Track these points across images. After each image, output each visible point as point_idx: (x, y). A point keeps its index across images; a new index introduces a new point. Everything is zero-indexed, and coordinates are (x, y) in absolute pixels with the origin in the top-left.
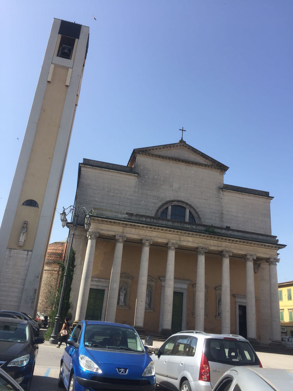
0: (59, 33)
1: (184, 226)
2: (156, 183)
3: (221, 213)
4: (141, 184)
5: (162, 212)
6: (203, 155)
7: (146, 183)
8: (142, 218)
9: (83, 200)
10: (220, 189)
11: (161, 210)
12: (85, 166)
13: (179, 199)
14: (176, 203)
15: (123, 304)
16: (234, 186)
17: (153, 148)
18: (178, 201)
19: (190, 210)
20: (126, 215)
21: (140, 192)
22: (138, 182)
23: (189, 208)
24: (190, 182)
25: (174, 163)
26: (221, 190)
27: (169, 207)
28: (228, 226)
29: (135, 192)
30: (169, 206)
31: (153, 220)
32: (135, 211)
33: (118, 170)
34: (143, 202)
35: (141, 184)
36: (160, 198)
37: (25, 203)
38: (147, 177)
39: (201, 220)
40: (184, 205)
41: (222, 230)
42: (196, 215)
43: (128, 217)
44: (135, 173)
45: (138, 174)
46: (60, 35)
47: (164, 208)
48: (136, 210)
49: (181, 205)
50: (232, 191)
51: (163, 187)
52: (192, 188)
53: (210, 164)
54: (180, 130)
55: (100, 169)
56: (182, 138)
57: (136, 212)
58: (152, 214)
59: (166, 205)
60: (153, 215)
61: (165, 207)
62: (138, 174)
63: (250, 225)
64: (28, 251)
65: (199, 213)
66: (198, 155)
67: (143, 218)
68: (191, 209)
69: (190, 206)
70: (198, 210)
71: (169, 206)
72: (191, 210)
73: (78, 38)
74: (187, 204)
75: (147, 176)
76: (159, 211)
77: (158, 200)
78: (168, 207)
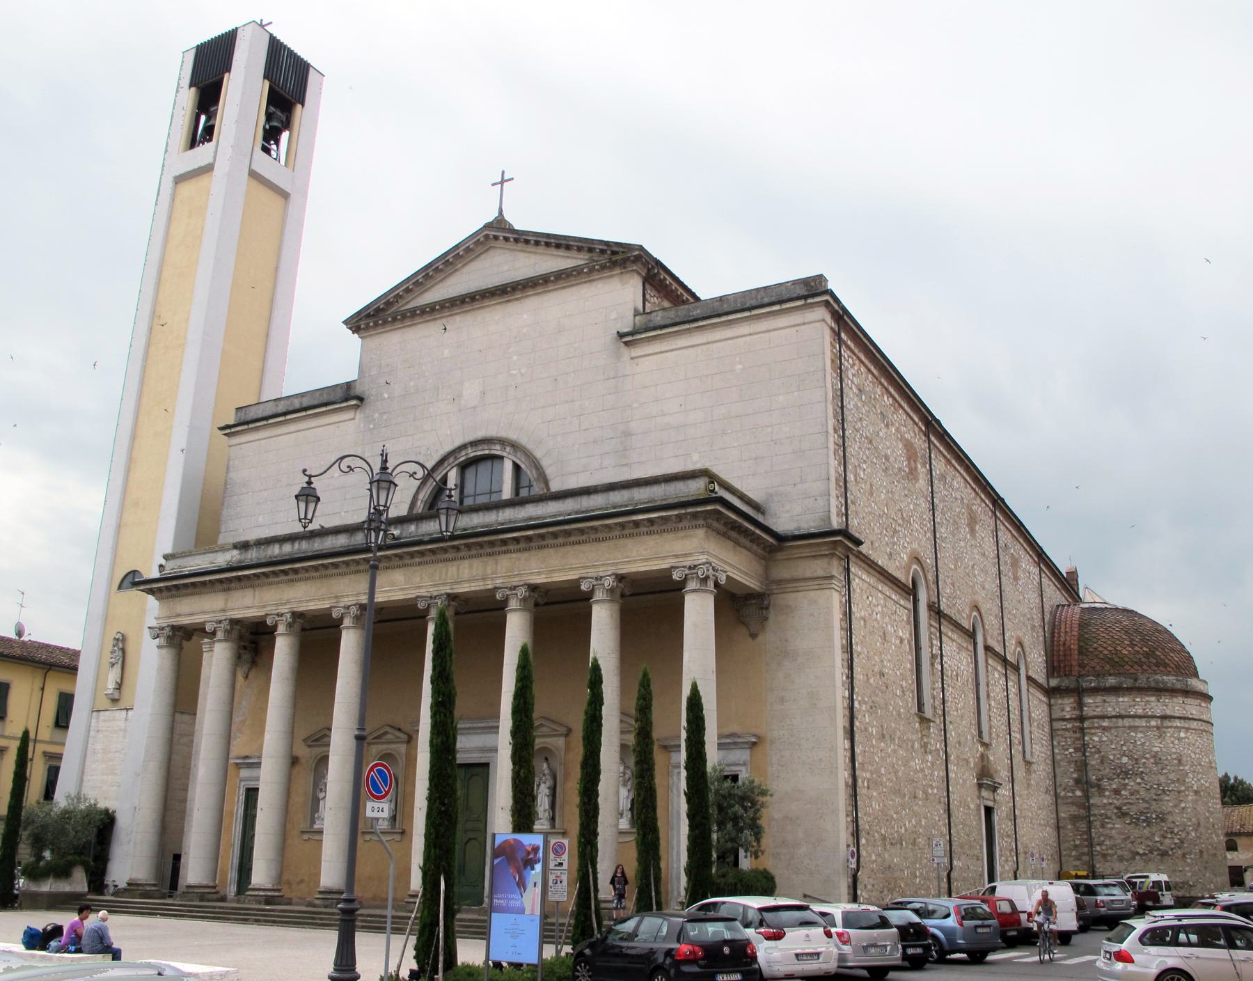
0: (191, 85)
6: (553, 241)
7: (385, 417)
8: (272, 547)
13: (480, 434)
14: (472, 453)
17: (397, 292)
18: (475, 444)
20: (235, 552)
23: (510, 456)
24: (515, 358)
25: (463, 312)
30: (448, 468)
33: (306, 409)
36: (422, 452)
37: (126, 583)
38: (386, 396)
40: (496, 450)
42: (534, 472)
43: (238, 557)
45: (361, 399)
46: (193, 89)
49: (487, 452)
50: (659, 332)
51: (431, 409)
53: (583, 259)
55: (265, 425)
59: (441, 469)
63: (735, 444)
65: (545, 463)
68: (519, 454)
69: (515, 446)
70: (538, 454)
74: (502, 442)
76: (417, 499)
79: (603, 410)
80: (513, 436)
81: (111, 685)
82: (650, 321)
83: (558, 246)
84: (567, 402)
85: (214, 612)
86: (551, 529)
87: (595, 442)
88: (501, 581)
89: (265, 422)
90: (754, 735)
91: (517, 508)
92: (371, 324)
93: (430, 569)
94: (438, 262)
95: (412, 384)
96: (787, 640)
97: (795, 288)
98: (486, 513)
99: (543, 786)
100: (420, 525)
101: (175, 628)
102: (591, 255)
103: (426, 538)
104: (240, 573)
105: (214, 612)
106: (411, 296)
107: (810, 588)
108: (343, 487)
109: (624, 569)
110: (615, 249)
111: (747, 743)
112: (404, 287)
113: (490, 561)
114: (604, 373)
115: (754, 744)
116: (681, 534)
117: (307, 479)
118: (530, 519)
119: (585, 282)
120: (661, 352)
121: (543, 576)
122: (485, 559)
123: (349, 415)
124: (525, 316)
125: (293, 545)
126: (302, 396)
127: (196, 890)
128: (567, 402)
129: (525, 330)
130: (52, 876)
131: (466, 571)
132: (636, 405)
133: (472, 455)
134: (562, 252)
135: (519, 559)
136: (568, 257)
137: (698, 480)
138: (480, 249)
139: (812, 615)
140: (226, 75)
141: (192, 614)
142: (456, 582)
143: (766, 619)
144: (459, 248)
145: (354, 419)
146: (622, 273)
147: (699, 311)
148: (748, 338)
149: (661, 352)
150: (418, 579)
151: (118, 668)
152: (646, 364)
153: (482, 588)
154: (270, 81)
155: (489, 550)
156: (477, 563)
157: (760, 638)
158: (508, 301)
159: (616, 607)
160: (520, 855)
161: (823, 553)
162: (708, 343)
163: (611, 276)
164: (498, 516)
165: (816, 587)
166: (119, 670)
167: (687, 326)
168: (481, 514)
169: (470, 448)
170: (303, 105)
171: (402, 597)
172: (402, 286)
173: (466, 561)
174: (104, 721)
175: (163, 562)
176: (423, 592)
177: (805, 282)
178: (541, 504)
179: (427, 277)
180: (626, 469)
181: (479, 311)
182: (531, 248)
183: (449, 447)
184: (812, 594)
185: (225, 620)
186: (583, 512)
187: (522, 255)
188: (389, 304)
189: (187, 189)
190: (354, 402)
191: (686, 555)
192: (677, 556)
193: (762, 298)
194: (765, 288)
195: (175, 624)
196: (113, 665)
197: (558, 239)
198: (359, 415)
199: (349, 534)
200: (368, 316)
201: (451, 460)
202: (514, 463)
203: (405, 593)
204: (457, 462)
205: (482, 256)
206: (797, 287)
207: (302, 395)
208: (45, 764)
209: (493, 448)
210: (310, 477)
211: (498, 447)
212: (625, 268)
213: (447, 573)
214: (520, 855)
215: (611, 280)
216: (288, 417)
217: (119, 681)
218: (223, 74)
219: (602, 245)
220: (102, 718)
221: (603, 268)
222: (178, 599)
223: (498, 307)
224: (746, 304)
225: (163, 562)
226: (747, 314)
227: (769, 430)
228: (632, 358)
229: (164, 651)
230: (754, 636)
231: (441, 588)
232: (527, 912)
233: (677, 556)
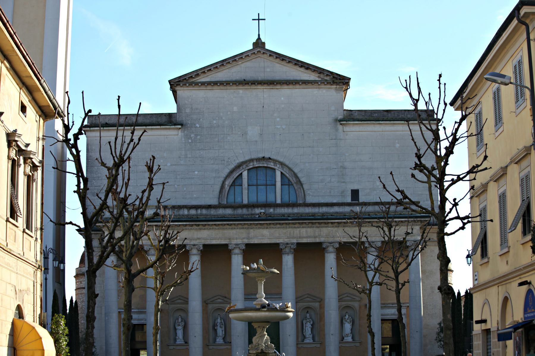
1: (253, 212)
2: (215, 133)
3: (341, 167)
4: (190, 141)
5: (233, 184)
7: (199, 137)
8: (182, 210)
9: (97, 188)
10: (338, 122)
11: (228, 182)
12: (91, 129)
14: (256, 164)
15: (183, 341)
16: (365, 111)
18: (258, 160)
19: (282, 171)
21: (189, 156)
23: (279, 169)
24: (278, 119)
26: (338, 123)
27: (243, 173)
28: (356, 188)
29: (180, 157)
30: (243, 170)
31: (201, 211)
32: (185, 191)
34: (196, 173)
35: (190, 141)
38: (197, 125)
39: (304, 186)
40: (271, 165)
41: (320, 208)
42: (294, 179)
44: (175, 125)
47: (235, 177)
48: (185, 189)
49: (266, 165)
50: (360, 122)
51: (229, 138)
52: (283, 129)
54: (253, 20)
56: (259, 35)
57: (186, 192)
58: (213, 191)
61: (236, 175)
62: (182, 125)
65: (299, 175)
66: (290, 65)
67: (184, 211)
69: (282, 164)
70: (296, 170)
71: (243, 170)
72: (284, 172)
74: (275, 161)
75: (198, 123)
77: (221, 164)
78: (241, 173)
79: (330, 154)
80: (281, 160)
82: (352, 114)
84: (310, 147)
88: (324, 239)
94: (230, 59)
95: (215, 122)
98: (313, 208)
100: (276, 209)
102: (319, 75)
106: (210, 73)
108: (174, 172)
114: (329, 136)
121: (345, 239)
125: (197, 211)
128: (310, 147)
129: (283, 106)
133: (257, 165)
136: (306, 73)
139: (432, 256)
142: (300, 238)
147: (376, 115)
153: (314, 241)
158: (272, 88)
168: (310, 208)
169: (255, 162)
172: (207, 68)
173: (304, 229)
180: (343, 184)
183: (242, 160)
190: (180, 127)
199: (233, 209)
201: (244, 166)
202: (281, 173)
204: (248, 168)
206: (423, 113)
209: (269, 163)
224: (399, 116)
231: (291, 240)
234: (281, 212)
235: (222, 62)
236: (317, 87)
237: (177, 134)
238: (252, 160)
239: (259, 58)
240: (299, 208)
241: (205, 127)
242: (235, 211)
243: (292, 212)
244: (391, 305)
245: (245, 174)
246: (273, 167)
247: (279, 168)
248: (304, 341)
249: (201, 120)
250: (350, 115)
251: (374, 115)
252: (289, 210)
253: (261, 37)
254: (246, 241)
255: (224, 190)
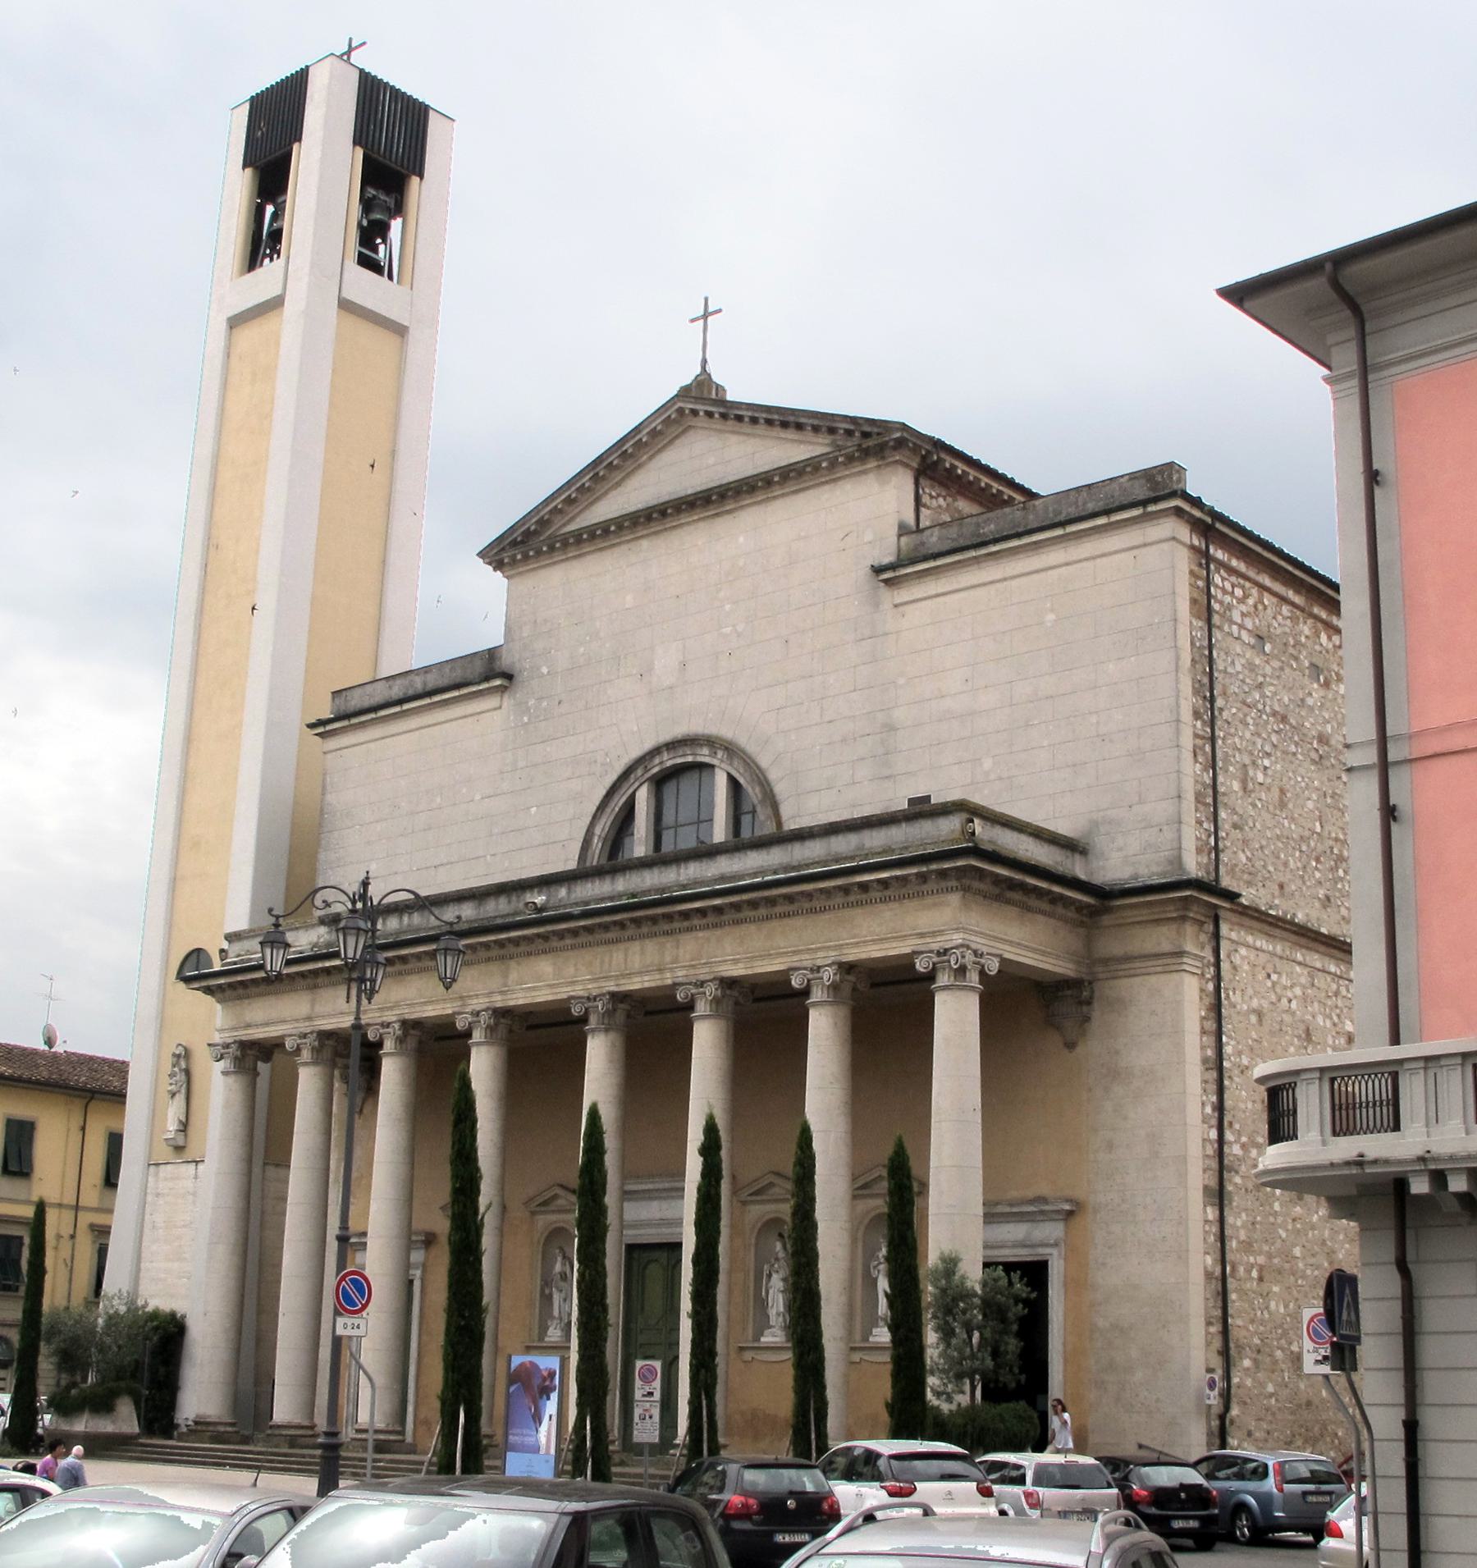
0: (245, 166)
6: (776, 417)
7: (545, 704)
11: (603, 827)
14: (669, 760)
18: (672, 745)
20: (323, 930)
21: (521, 764)
22: (512, 718)
23: (723, 765)
30: (637, 784)
34: (534, 810)
35: (526, 719)
38: (545, 670)
40: (704, 755)
42: (757, 790)
43: (327, 937)
45: (509, 677)
46: (249, 171)
49: (690, 759)
51: (609, 692)
53: (822, 444)
55: (373, 719)
56: (704, 362)
59: (626, 785)
60: (572, 865)
61: (620, 801)
64: (197, 1162)
65: (773, 775)
69: (731, 750)
70: (764, 761)
71: (637, 784)
73: (300, 140)
74: (711, 742)
76: (593, 834)
80: (726, 732)
81: (172, 1126)
83: (785, 425)
85: (297, 1020)
86: (745, 897)
87: (844, 740)
89: (373, 716)
90: (1068, 1200)
91: (704, 860)
92: (519, 557)
93: (587, 955)
94: (611, 455)
96: (1117, 1052)
97: (1132, 485)
98: (663, 869)
99: (775, 1276)
101: (245, 1046)
102: (832, 437)
103: (577, 910)
104: (327, 964)
105: (297, 1020)
107: (1153, 969)
109: (852, 955)
110: (867, 429)
111: (1058, 1212)
112: (563, 497)
113: (669, 943)
115: (1070, 1213)
116: (929, 900)
117: (273, 920)
118: (723, 878)
119: (827, 482)
120: (937, 595)
121: (741, 965)
122: (662, 939)
123: (491, 702)
124: (741, 539)
126: (426, 672)
127: (284, 1432)
129: (741, 563)
130: (87, 1410)
131: (637, 958)
132: (901, 681)
133: (669, 763)
134: (791, 434)
135: (708, 939)
136: (801, 442)
137: (951, 817)
138: (675, 430)
139: (1153, 1013)
140: (295, 146)
141: (267, 1024)
142: (623, 976)
143: (1087, 1019)
144: (640, 432)
145: (500, 707)
146: (879, 467)
147: (992, 526)
148: (1063, 570)
149: (937, 595)
150: (572, 970)
151: (180, 1099)
152: (917, 615)
153: (659, 983)
154: (365, 147)
155: (666, 927)
156: (651, 946)
157: (1079, 1049)
158: (717, 515)
159: (843, 1012)
160: (536, 1382)
161: (1169, 915)
162: (1005, 579)
163: (864, 472)
164: (679, 875)
165: (1159, 969)
166: (183, 1104)
167: (972, 553)
168: (656, 871)
169: (665, 754)
170: (421, 176)
171: (550, 998)
172: (560, 495)
173: (637, 943)
174: (166, 1179)
175: (225, 945)
176: (578, 990)
177: (1148, 475)
178: (737, 855)
179: (596, 478)
181: (674, 532)
182: (746, 427)
183: (636, 752)
184: (1153, 979)
185: (311, 1033)
186: (794, 868)
187: (734, 439)
188: (543, 523)
189: (249, 335)
190: (498, 682)
191: (934, 934)
192: (922, 935)
193: (1084, 504)
194: (1089, 486)
195: (244, 1038)
196: (173, 1095)
197: (783, 414)
198: (508, 701)
199: (476, 902)
200: (514, 543)
201: (639, 772)
202: (731, 779)
203: (555, 990)
205: (678, 442)
206: (1137, 483)
207: (426, 670)
208: (94, 1242)
209: (699, 751)
210: (277, 917)
211: (705, 751)
212: (883, 458)
213: (610, 961)
214: (536, 1382)
215: (864, 477)
216: (406, 707)
217: (184, 1120)
218: (290, 145)
219: (847, 422)
220: (161, 1175)
221: (850, 459)
222: (247, 1001)
223: (701, 525)
224: (1060, 513)
225: (225, 945)
226: (1059, 532)
227: (1094, 719)
228: (896, 606)
229: (231, 1079)
230: (1071, 1046)
231: (603, 984)
232: (542, 1451)
233: (922, 935)
234: (585, 893)
235: (593, 469)
236: (827, 478)
237: (498, 705)
238: (656, 751)
239: (691, 433)
240: (627, 877)
241: (559, 670)
242: (482, 909)
243: (610, 889)
244: (1008, 1209)
245: (643, 797)
246: (707, 760)
247: (722, 761)
248: (762, 1339)
249: (553, 651)
250: (916, 548)
251: (986, 530)
252: (605, 886)
253: (710, 368)
254: (499, 1001)
255: (590, 852)
